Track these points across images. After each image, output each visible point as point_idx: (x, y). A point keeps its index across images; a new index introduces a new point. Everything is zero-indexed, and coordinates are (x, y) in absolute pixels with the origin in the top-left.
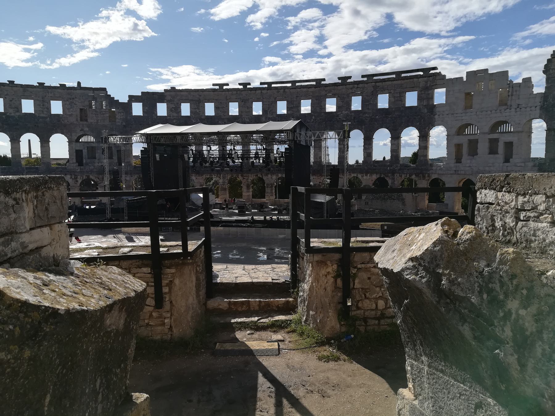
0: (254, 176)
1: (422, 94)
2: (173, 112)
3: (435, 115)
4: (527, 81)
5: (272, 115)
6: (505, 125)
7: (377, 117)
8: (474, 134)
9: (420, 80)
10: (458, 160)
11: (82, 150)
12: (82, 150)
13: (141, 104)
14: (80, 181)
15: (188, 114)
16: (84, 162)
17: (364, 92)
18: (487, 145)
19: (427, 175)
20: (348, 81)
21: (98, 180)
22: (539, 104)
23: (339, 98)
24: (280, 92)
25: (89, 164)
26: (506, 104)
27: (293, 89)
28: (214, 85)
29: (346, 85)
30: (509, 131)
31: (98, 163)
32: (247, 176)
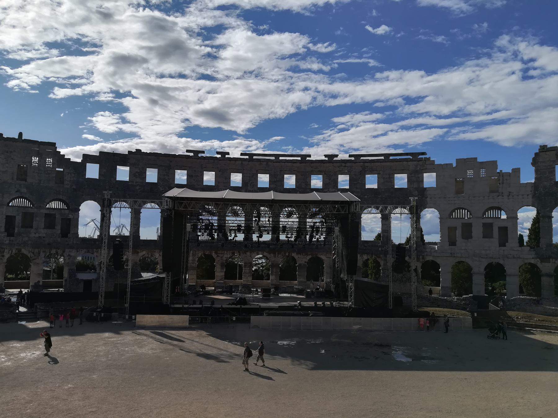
1: (412, 177)
3: (427, 198)
4: (517, 171)
5: (253, 187)
6: (489, 211)
7: (366, 196)
8: (462, 218)
9: (410, 163)
10: (453, 243)
11: (15, 217)
12: (15, 217)
13: (97, 166)
14: (7, 256)
16: (16, 231)
17: (352, 171)
18: (481, 229)
19: (421, 257)
20: (334, 159)
21: (32, 255)
22: (530, 192)
23: (325, 175)
24: (262, 164)
25: (23, 235)
26: (497, 191)
27: (276, 162)
28: (188, 151)
29: (333, 163)
30: (497, 216)
31: (35, 234)
32: (222, 254)
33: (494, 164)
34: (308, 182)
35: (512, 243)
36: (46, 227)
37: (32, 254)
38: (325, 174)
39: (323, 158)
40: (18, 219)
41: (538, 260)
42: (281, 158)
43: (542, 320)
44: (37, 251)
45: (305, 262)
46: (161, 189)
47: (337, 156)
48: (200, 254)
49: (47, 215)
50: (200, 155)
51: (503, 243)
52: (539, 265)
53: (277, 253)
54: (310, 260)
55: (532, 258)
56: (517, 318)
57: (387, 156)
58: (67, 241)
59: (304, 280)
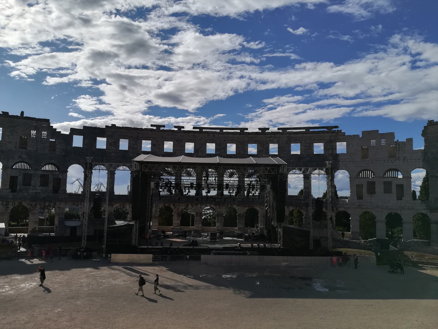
0: (185, 205)
1: (327, 145)
2: (112, 146)
3: (339, 161)
4: (410, 141)
7: (292, 161)
9: (325, 134)
10: (360, 197)
11: (17, 177)
12: (17, 177)
13: (82, 137)
14: (11, 208)
15: (127, 149)
16: (18, 188)
19: (335, 208)
20: (266, 132)
21: (30, 207)
28: (152, 126)
29: (265, 135)
31: (33, 190)
33: (392, 135)
34: (245, 150)
35: (407, 197)
36: (41, 185)
37: (30, 206)
38: (259, 143)
39: (257, 130)
40: (20, 179)
41: (429, 211)
42: (224, 131)
43: (432, 259)
44: (34, 204)
45: (244, 212)
46: (131, 155)
47: (268, 129)
48: (161, 206)
49: (42, 176)
50: (162, 128)
51: (400, 197)
52: (429, 214)
53: (221, 205)
54: (247, 210)
55: (423, 209)
56: (412, 257)
57: (307, 129)
58: (57, 196)
59: (243, 227)
